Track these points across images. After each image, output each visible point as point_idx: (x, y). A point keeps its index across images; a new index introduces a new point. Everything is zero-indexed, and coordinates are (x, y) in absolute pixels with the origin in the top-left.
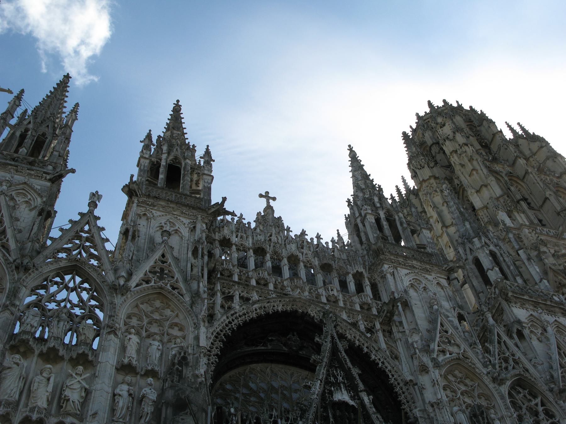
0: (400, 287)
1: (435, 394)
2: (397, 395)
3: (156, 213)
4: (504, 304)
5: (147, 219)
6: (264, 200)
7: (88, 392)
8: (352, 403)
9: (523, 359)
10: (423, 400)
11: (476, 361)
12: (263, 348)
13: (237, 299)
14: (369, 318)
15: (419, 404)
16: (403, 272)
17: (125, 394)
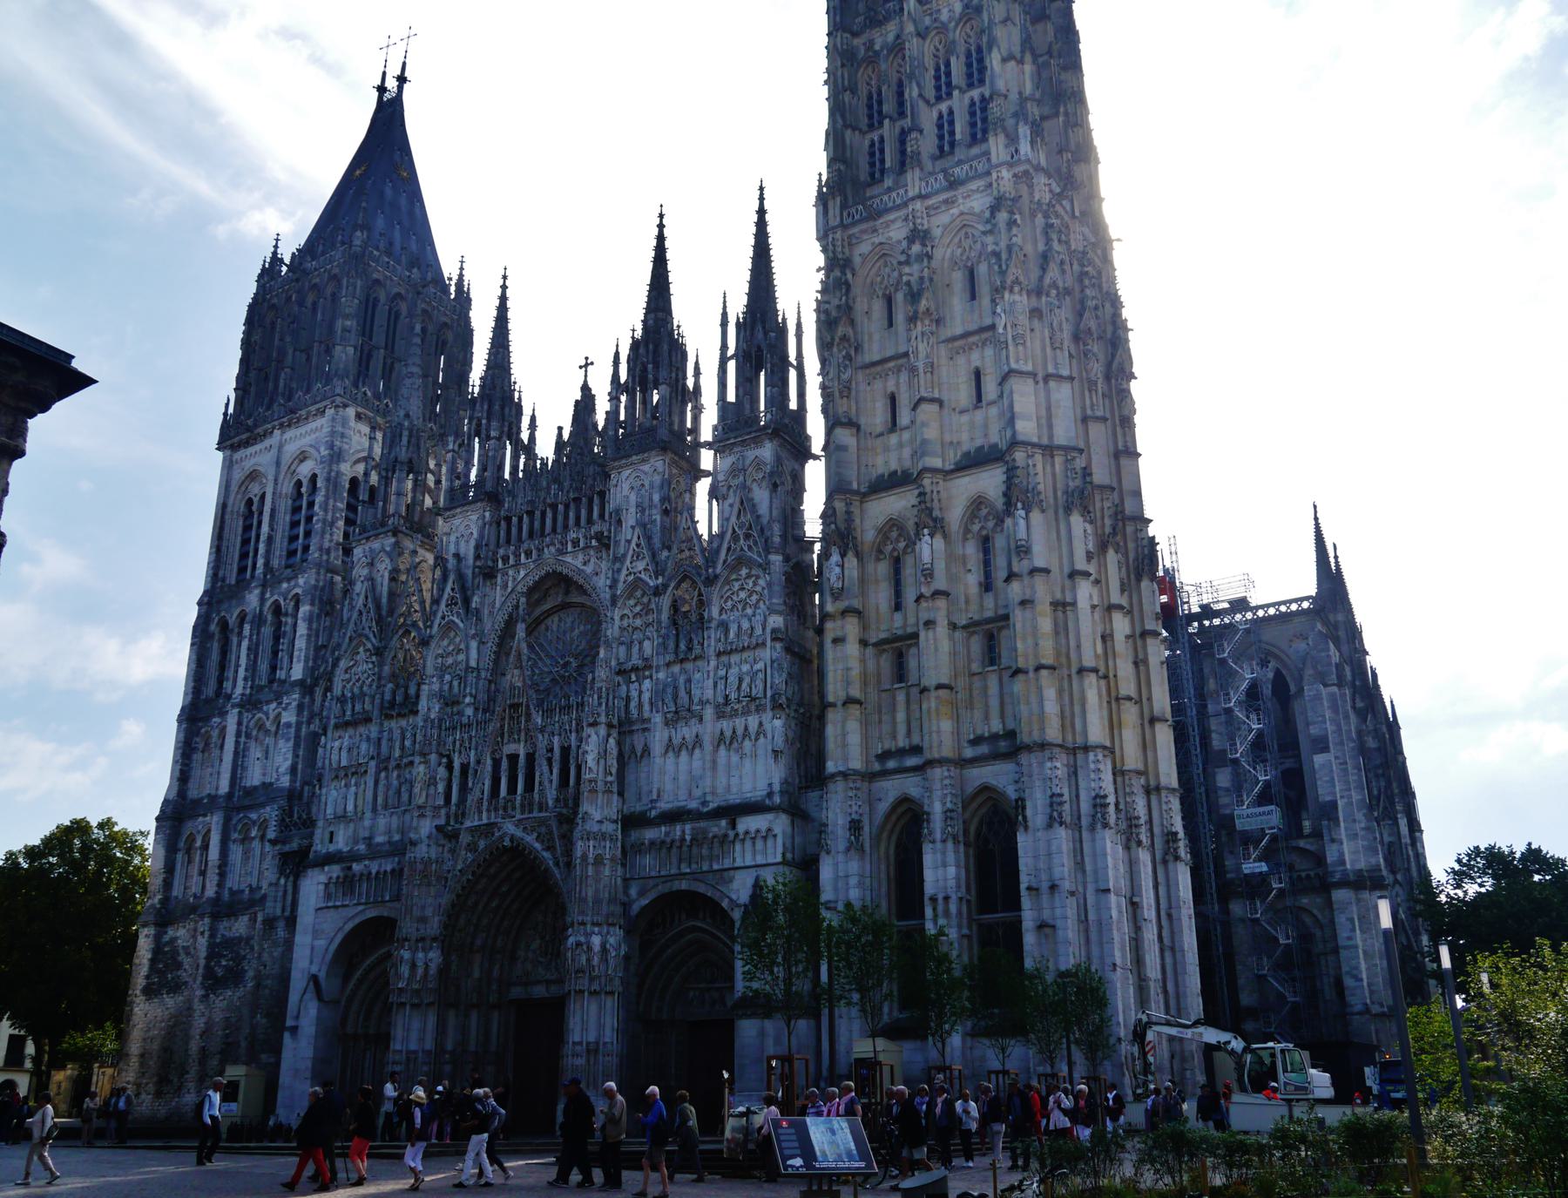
3: (457, 522)
13: (510, 584)
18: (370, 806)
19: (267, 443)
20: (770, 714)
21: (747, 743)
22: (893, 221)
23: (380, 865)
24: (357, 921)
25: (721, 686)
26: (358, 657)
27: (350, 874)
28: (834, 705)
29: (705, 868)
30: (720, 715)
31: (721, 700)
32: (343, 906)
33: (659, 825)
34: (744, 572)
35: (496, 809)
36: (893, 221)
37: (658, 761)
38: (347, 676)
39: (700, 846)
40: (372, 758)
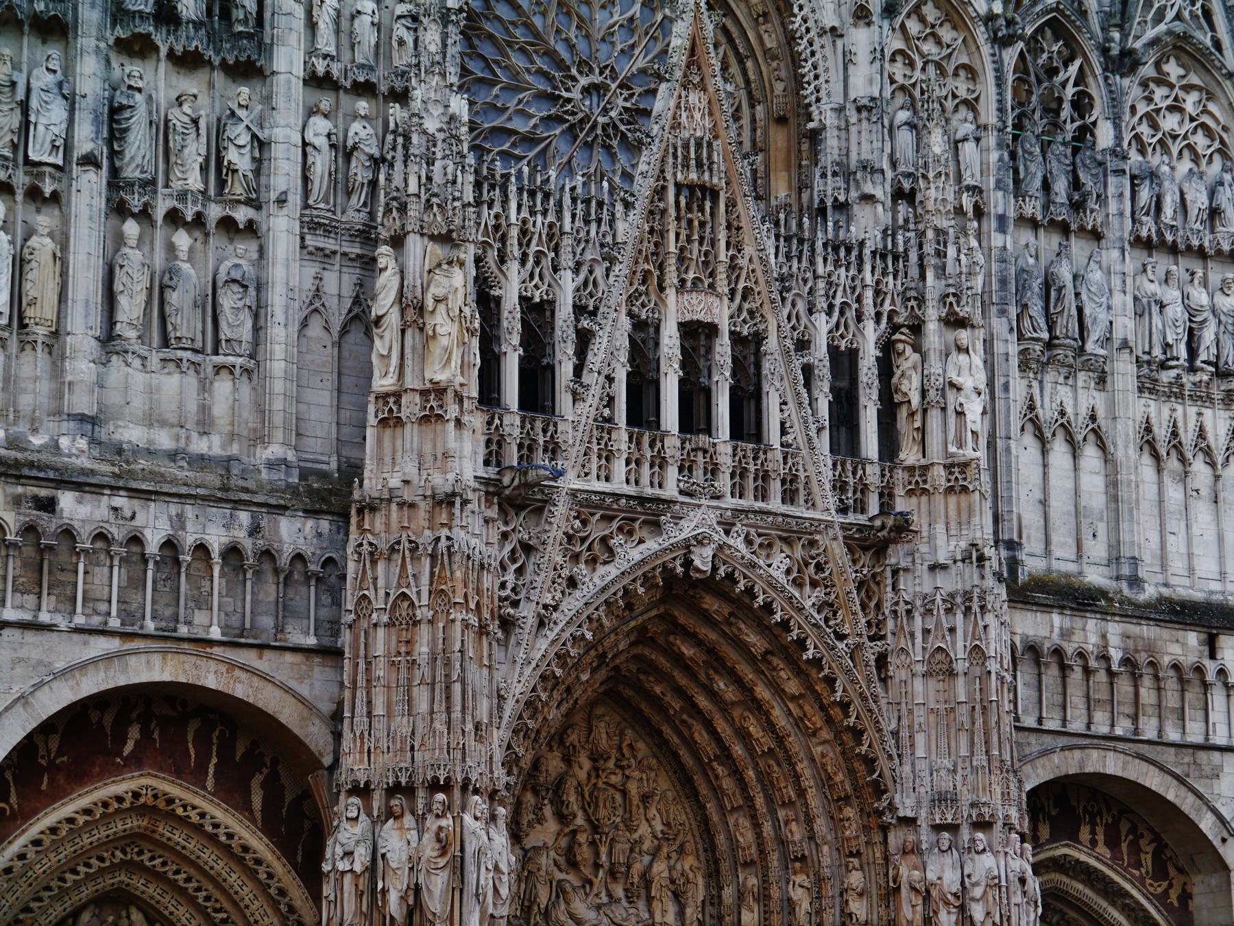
1: (871, 81)
7: (261, 144)
17: (321, 142)
18: (96, 319)
21: (1199, 466)
23: (179, 522)
24: (91, 684)
25: (1157, 320)
27: (49, 524)
29: (1150, 733)
30: (1147, 387)
31: (1157, 352)
32: (23, 626)
33: (1047, 608)
34: (1173, 70)
35: (660, 462)
37: (1013, 444)
39: (1136, 679)
40: (89, 160)
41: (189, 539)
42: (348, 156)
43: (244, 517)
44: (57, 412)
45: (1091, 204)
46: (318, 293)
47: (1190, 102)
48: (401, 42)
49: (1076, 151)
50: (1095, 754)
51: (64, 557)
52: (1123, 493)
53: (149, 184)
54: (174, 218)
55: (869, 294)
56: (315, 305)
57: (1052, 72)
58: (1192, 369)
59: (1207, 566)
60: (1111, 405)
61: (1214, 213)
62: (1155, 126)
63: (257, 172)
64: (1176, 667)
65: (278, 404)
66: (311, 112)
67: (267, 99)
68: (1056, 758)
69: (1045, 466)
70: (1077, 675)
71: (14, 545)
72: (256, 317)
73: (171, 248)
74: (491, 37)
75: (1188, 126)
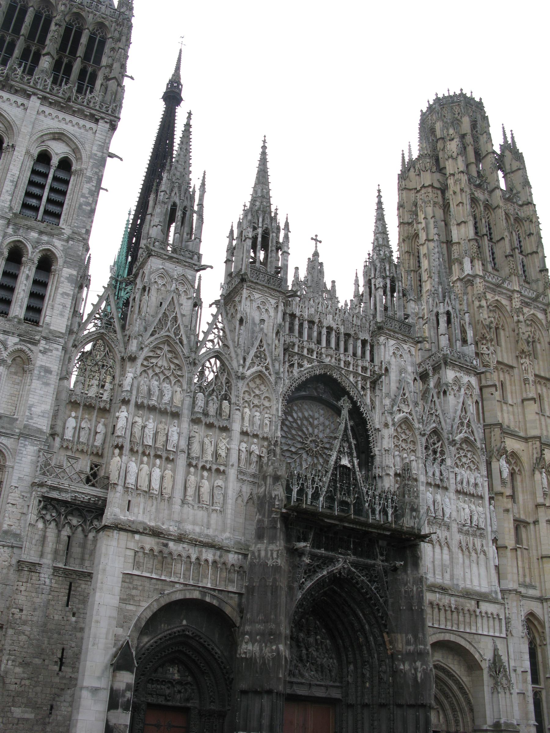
0: (388, 358)
1: (389, 443)
2: (368, 436)
3: (257, 296)
4: (443, 366)
5: (251, 300)
6: (314, 242)
8: (349, 466)
9: (441, 416)
10: (382, 443)
11: (415, 418)
12: (304, 393)
13: (296, 365)
14: (364, 379)
15: (379, 444)
16: (392, 342)
17: (244, 449)
19: (20, 100)
20: (491, 542)
21: (473, 554)
22: (503, 293)
26: (159, 352)
27: (166, 550)
28: (506, 547)
30: (460, 531)
31: (463, 521)
33: (435, 592)
34: (464, 446)
36: (503, 293)
38: (145, 363)
39: (458, 613)
41: (204, 557)
42: (251, 454)
43: (218, 553)
44: (169, 519)
45: (445, 480)
46: (241, 491)
47: (469, 455)
48: (266, 424)
49: (441, 465)
50: (447, 634)
51: (169, 560)
52: (455, 561)
53: (198, 458)
54: (204, 468)
55: (390, 500)
56: (240, 494)
57: (434, 444)
58: (471, 527)
59: (476, 583)
60: (451, 535)
61: (476, 485)
62: (460, 460)
63: (226, 457)
64: (469, 610)
65: (229, 521)
66: (241, 441)
67: (230, 437)
68: (437, 635)
69: (434, 552)
70: (442, 612)
71: (156, 556)
72: (224, 497)
73: (202, 477)
74: (286, 425)
75: (469, 461)
